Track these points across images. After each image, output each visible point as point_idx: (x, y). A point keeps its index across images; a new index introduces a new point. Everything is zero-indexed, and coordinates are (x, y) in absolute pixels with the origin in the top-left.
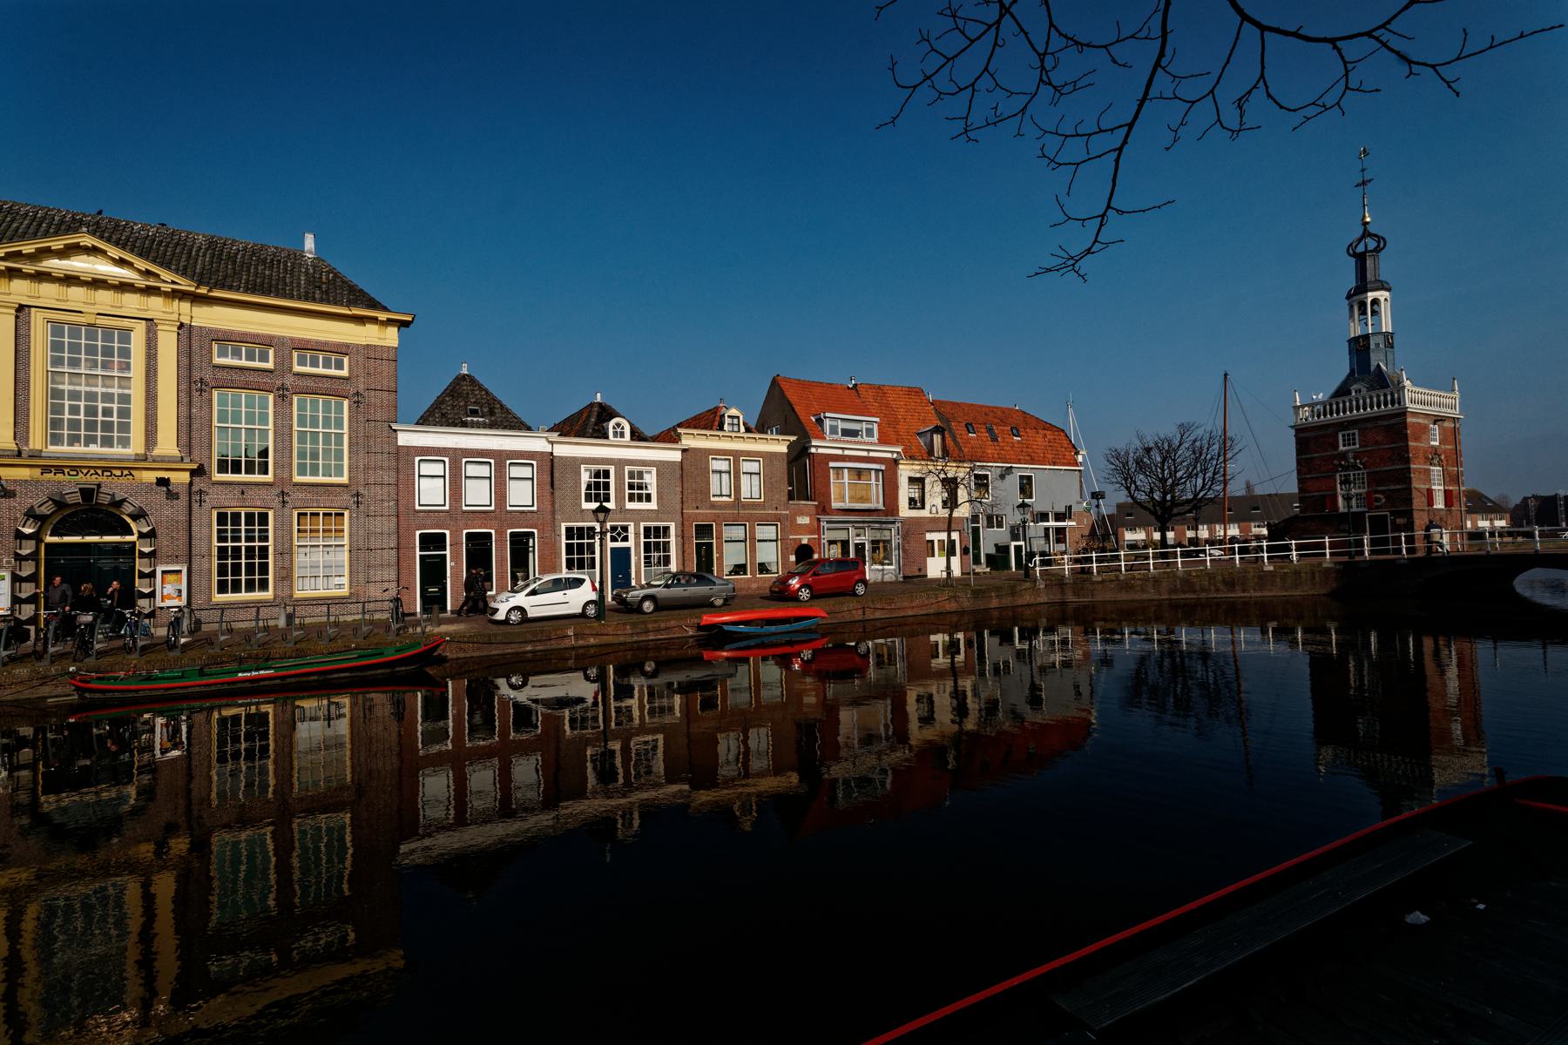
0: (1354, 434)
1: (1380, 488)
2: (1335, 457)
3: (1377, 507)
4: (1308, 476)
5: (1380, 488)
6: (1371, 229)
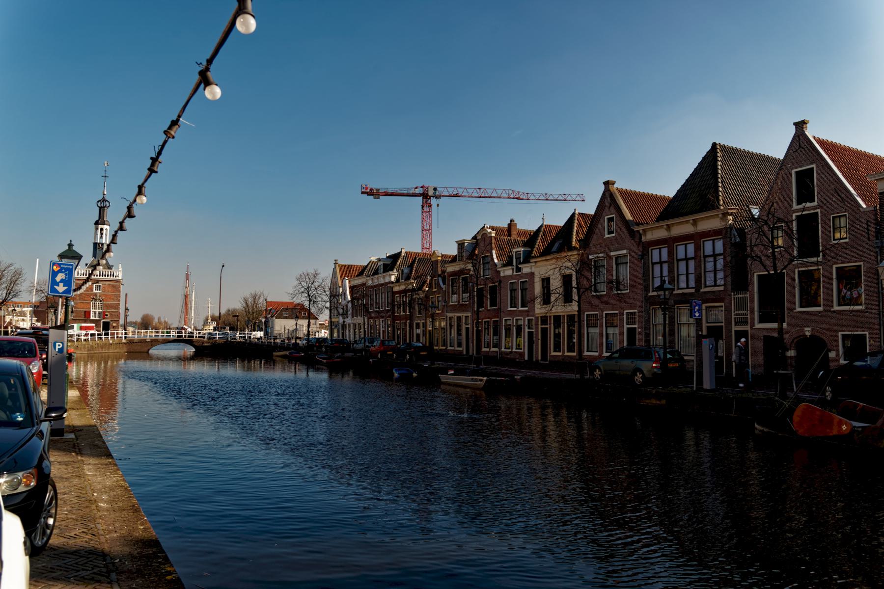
0: (100, 286)
1: (108, 310)
2: (92, 294)
3: (107, 318)
4: (79, 301)
5: (108, 310)
6: (106, 198)
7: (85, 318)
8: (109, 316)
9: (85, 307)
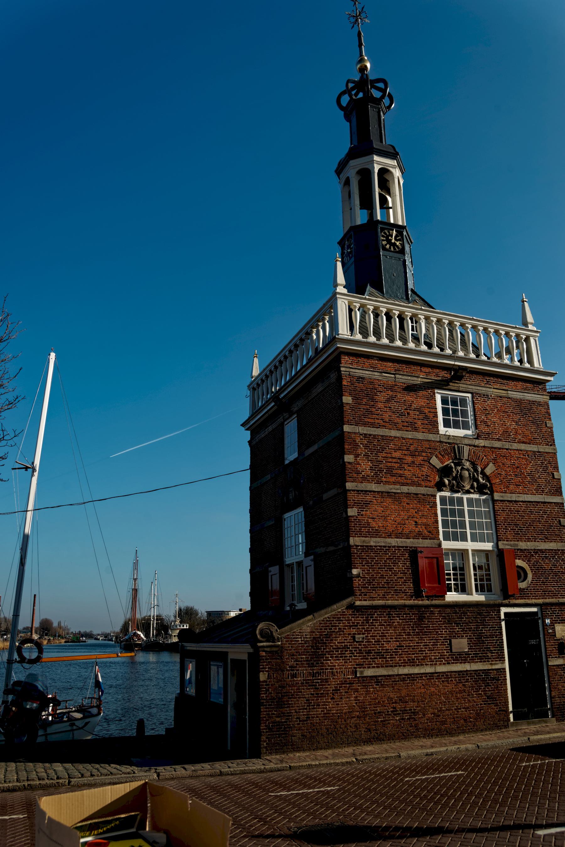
3: (523, 593)
4: (373, 487)
5: (523, 545)
7: (418, 594)
8: (530, 576)
9: (410, 526)
